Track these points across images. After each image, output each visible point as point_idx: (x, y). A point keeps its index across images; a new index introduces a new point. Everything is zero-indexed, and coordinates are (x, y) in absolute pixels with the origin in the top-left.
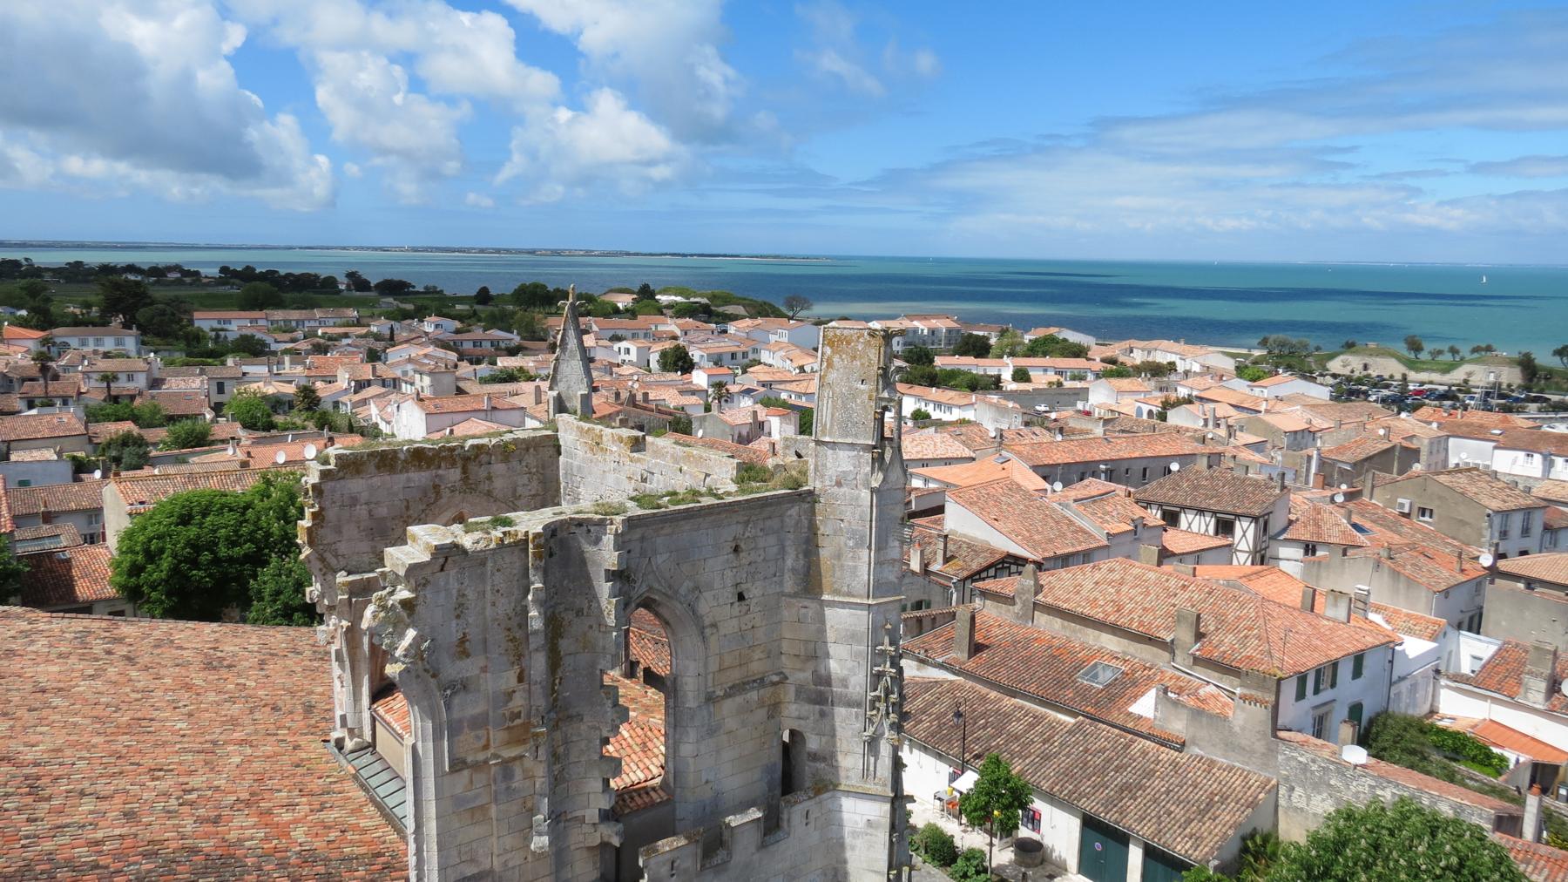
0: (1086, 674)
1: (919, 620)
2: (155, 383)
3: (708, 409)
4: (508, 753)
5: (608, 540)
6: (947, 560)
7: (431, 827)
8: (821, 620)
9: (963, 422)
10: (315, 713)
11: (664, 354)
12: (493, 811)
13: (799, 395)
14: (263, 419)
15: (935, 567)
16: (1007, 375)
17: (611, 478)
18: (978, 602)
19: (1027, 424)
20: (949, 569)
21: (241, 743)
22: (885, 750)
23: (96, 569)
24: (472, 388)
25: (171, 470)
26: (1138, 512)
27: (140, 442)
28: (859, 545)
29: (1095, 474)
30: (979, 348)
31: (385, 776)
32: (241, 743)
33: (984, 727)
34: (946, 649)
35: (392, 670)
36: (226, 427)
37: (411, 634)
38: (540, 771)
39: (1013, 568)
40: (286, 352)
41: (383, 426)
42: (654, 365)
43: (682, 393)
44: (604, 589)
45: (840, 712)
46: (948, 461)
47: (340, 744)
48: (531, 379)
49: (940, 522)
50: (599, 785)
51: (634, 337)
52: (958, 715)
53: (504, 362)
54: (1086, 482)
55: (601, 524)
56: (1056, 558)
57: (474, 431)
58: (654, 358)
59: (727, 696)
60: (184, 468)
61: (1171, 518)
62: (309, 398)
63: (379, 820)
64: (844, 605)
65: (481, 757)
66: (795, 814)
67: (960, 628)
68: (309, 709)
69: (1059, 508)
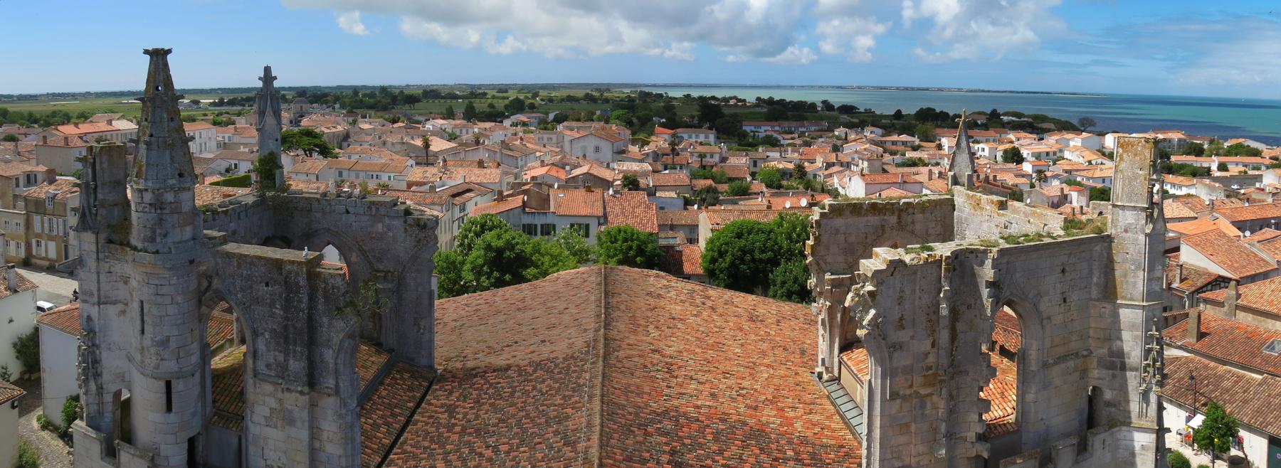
1: (1166, 318)
2: (724, 160)
3: (1032, 186)
4: (923, 392)
5: (989, 263)
6: (1182, 281)
7: (877, 433)
8: (1116, 316)
9: (1189, 195)
10: (807, 356)
11: (1005, 152)
12: (913, 427)
13: (1088, 179)
14: (777, 182)
15: (1175, 285)
16: (1214, 167)
17: (985, 226)
18: (1202, 306)
19: (1228, 196)
20: (1184, 286)
21: (768, 366)
22: (1153, 398)
23: (695, 256)
24: (892, 169)
25: (730, 207)
27: (715, 191)
28: (1137, 268)
30: (1199, 151)
31: (845, 399)
32: (768, 366)
33: (1207, 385)
34: (1183, 337)
35: (861, 333)
36: (758, 186)
37: (872, 312)
38: (942, 405)
40: (789, 145)
41: (840, 190)
42: (999, 158)
43: (1017, 176)
44: (985, 292)
45: (1128, 374)
46: (1181, 220)
47: (820, 376)
48: (926, 165)
49: (1177, 257)
50: (976, 417)
51: (987, 141)
52: (1192, 378)
53: (910, 155)
55: (985, 252)
56: (1247, 277)
57: (893, 193)
58: (999, 155)
59: (1056, 363)
60: (736, 207)
62: (801, 171)
63: (842, 425)
64: (1128, 306)
65: (908, 392)
66: (1096, 441)
67: (1191, 323)
68: (803, 352)
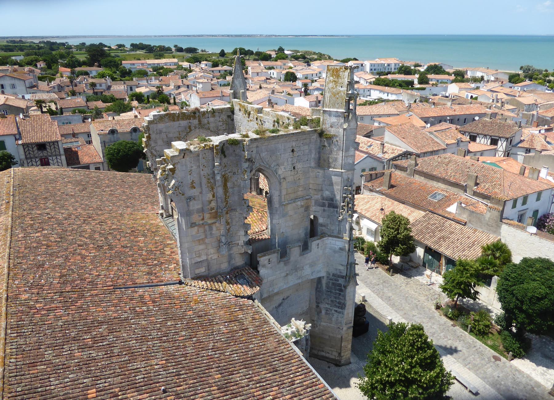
0: (432, 196)
26: (460, 136)
29: (445, 121)
39: (409, 156)
54: (441, 124)
61: (473, 138)
69: (428, 134)
